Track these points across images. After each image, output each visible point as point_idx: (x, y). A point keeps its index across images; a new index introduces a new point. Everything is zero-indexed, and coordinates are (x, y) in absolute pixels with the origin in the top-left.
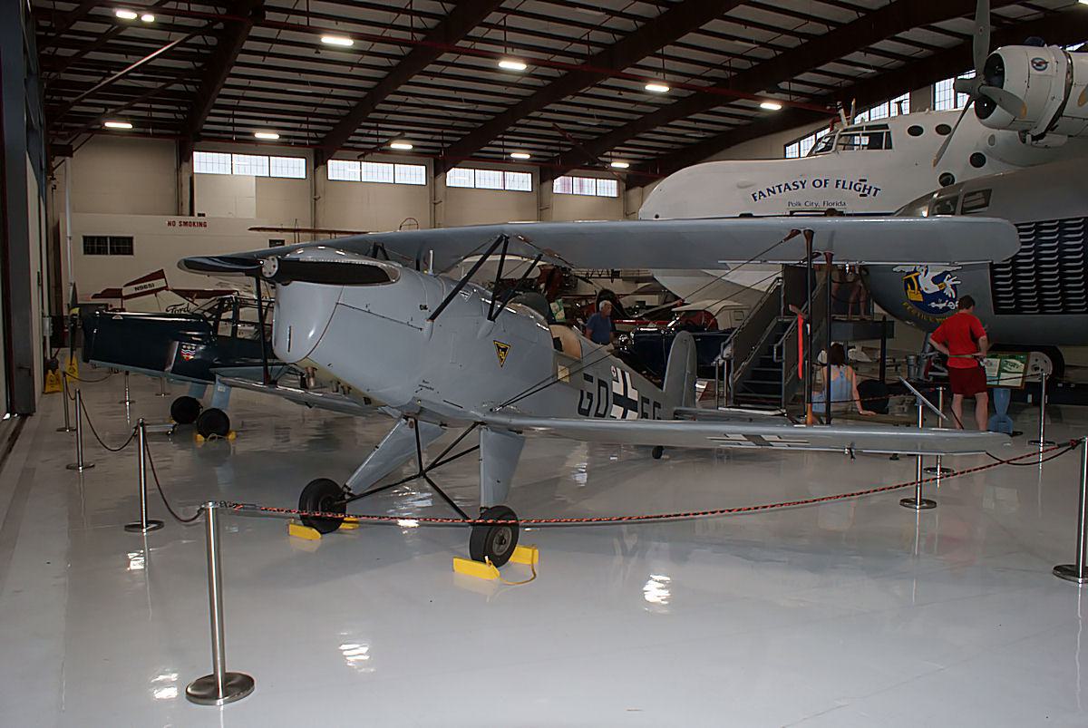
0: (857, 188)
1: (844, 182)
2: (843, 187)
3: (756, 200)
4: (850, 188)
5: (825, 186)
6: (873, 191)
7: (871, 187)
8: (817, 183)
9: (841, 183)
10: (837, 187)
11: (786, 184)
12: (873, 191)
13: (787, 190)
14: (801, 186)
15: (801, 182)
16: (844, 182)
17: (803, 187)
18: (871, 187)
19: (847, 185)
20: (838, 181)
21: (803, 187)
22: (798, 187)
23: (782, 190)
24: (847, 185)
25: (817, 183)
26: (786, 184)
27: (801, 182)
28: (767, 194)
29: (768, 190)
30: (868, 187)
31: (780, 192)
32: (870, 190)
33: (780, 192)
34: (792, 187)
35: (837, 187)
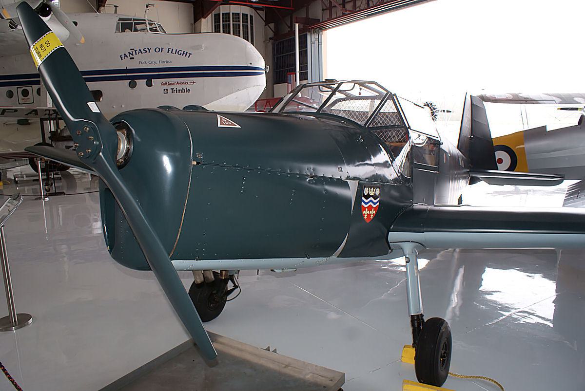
0: (180, 54)
1: (173, 49)
2: (172, 53)
3: (122, 59)
4: (176, 53)
5: (162, 52)
6: (188, 55)
7: (187, 53)
8: (157, 50)
9: (171, 50)
10: (168, 52)
11: (140, 50)
12: (188, 55)
13: (140, 53)
14: (148, 51)
15: (148, 49)
16: (173, 49)
17: (149, 52)
18: (187, 53)
19: (174, 52)
20: (169, 49)
21: (149, 52)
22: (146, 51)
23: (137, 53)
24: (174, 52)
25: (157, 50)
26: (125, 54)
27: (148, 49)
28: (128, 56)
29: (129, 53)
30: (185, 53)
31: (136, 54)
32: (186, 54)
33: (136, 54)
34: (143, 51)
35: (168, 52)
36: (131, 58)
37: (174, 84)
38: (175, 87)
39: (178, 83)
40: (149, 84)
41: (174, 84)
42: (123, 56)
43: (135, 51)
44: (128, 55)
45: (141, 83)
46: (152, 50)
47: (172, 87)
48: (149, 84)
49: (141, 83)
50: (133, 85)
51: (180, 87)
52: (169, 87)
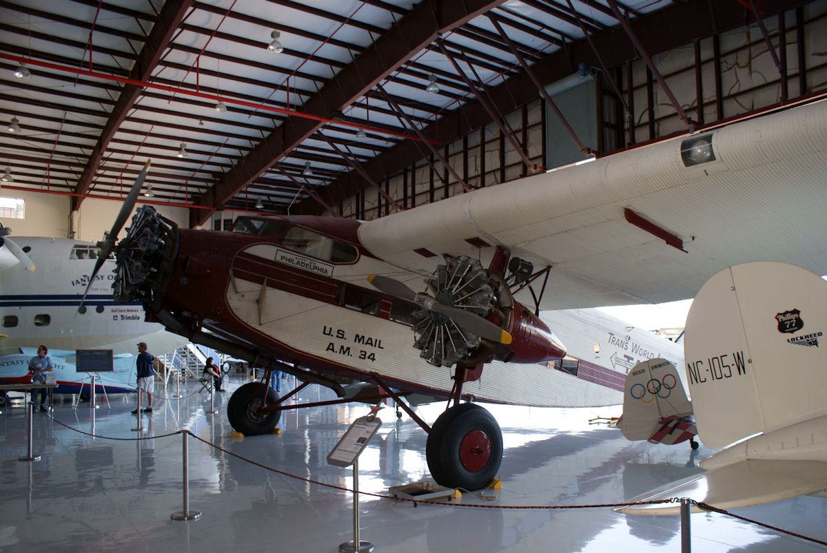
14: (101, 278)
29: (82, 280)
36: (83, 285)
37: (124, 311)
38: (125, 314)
39: (128, 310)
40: (100, 310)
41: (124, 311)
42: (75, 282)
43: (88, 278)
44: (80, 281)
45: (92, 309)
46: (105, 278)
47: (122, 314)
48: (100, 310)
49: (92, 309)
50: (83, 311)
51: (130, 314)
52: (119, 314)
